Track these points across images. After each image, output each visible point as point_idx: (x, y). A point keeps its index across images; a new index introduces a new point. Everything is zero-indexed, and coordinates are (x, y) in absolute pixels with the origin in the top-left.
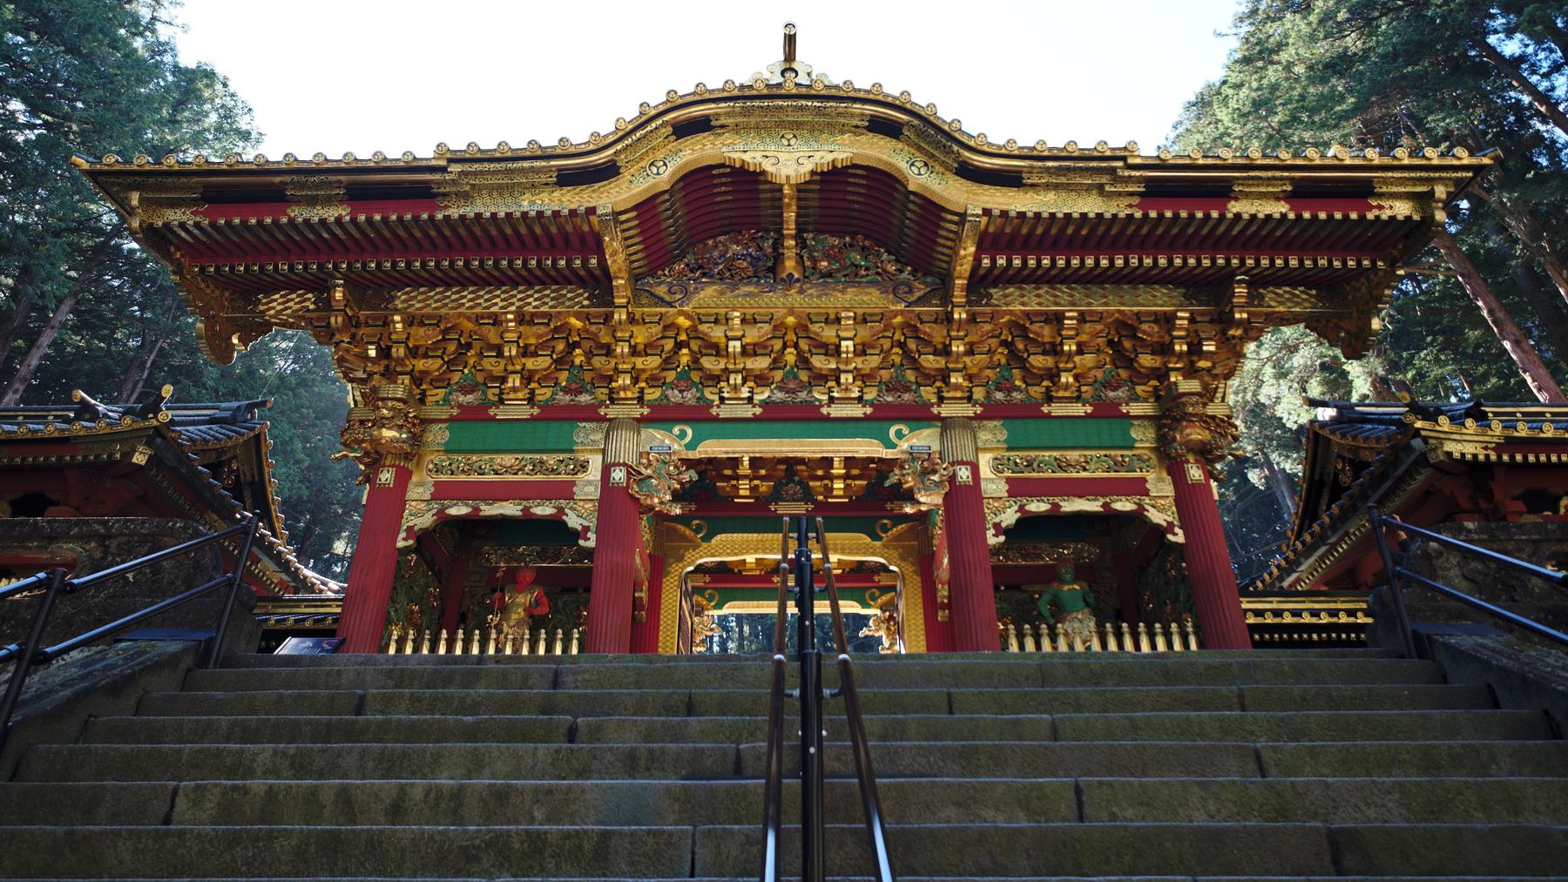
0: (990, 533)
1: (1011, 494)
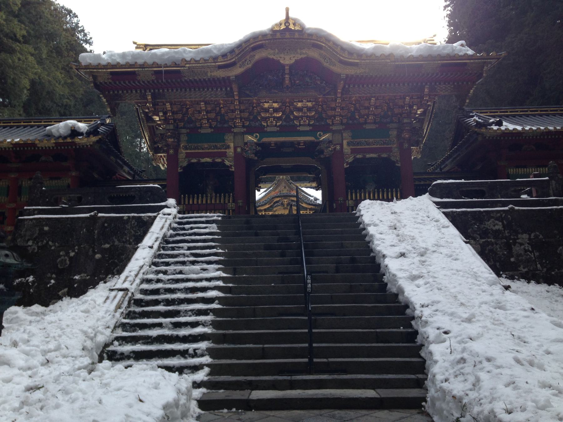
0: (345, 164)
1: (352, 153)
